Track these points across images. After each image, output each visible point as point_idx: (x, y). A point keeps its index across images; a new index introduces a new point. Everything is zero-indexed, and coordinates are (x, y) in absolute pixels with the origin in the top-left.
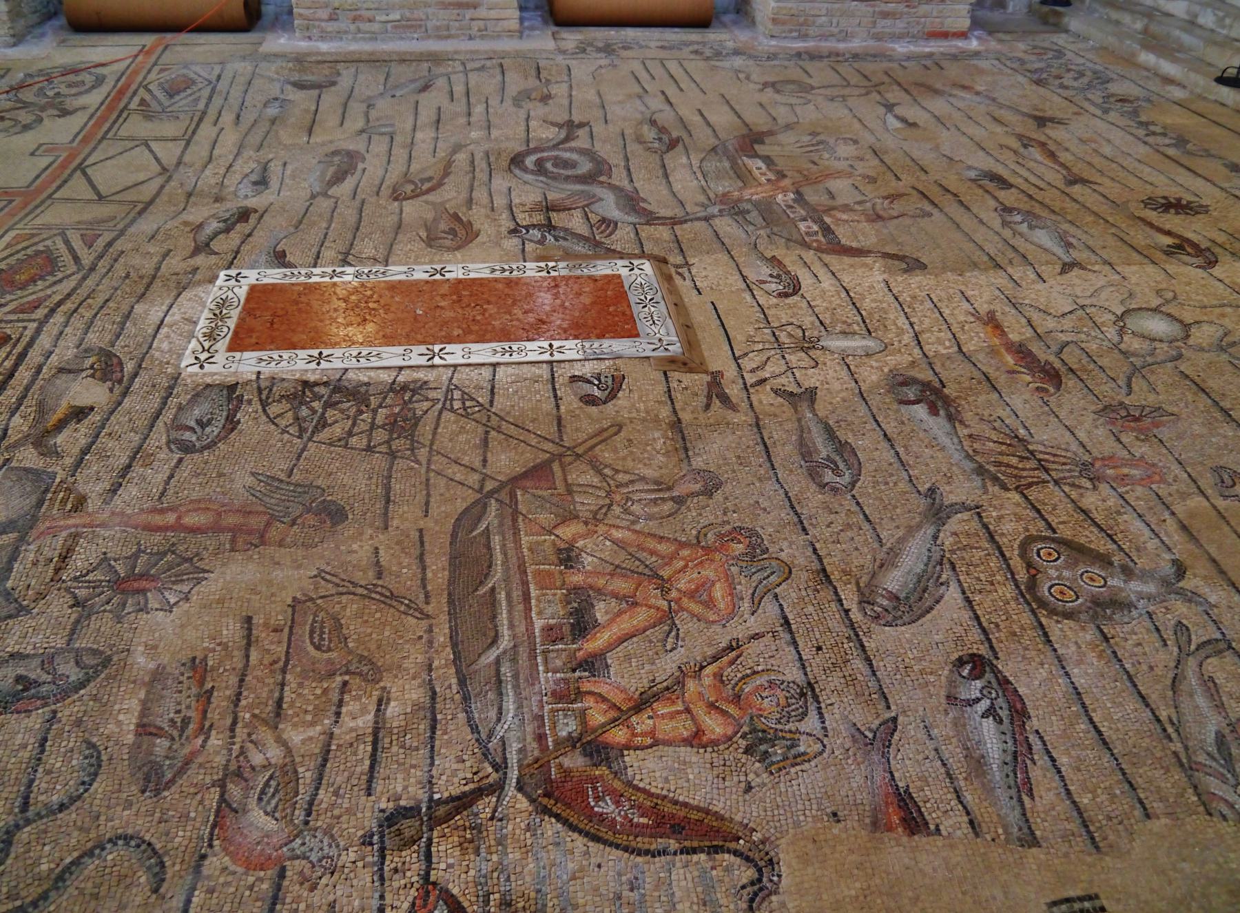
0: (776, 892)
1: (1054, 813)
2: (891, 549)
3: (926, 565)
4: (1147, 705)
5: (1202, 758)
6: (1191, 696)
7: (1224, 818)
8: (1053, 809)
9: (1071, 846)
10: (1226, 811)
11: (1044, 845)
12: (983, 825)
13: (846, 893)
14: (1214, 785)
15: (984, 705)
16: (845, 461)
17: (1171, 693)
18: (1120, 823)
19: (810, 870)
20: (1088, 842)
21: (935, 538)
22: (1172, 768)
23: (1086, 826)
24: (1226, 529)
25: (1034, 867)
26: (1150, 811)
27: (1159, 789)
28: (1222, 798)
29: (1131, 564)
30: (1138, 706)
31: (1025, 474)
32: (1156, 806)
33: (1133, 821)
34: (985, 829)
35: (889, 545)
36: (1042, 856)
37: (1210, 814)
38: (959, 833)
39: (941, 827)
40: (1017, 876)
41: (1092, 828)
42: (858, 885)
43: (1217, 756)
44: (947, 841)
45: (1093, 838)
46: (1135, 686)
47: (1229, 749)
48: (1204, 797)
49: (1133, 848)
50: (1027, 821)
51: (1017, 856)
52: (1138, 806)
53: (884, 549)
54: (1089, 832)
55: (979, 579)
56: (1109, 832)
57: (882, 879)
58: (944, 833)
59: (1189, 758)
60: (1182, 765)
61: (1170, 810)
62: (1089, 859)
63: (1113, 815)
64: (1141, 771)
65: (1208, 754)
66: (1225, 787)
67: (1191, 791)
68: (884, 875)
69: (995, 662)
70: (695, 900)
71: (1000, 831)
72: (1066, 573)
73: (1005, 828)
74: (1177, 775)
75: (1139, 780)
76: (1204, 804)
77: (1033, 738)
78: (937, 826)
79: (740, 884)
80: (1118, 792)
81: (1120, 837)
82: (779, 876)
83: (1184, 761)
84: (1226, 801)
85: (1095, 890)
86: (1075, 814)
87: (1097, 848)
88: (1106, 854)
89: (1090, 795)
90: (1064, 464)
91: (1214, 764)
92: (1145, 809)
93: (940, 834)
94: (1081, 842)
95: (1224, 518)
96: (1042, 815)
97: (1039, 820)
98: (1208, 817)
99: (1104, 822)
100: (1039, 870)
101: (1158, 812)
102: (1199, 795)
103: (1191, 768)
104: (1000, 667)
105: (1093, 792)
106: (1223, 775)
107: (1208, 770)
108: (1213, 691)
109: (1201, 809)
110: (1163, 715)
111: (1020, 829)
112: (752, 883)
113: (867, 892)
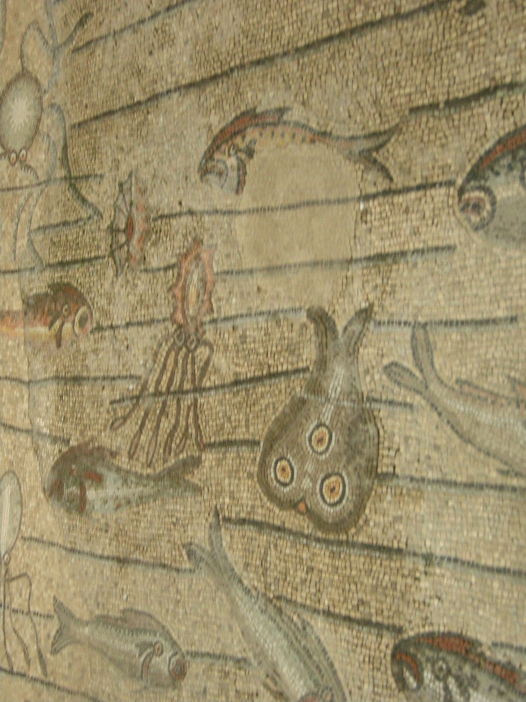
2: (255, 656)
3: (280, 629)
4: (481, 487)
6: (478, 424)
15: (452, 683)
16: (145, 631)
17: (469, 448)
21: (248, 592)
24: (278, 216)
29: (308, 375)
30: (480, 500)
31: (182, 423)
35: (250, 655)
46: (455, 484)
53: (255, 663)
55: (304, 581)
69: (405, 636)
72: (309, 467)
77: (500, 656)
90: (176, 362)
95: (263, 210)
104: (411, 633)
108: (475, 393)
110: (494, 477)
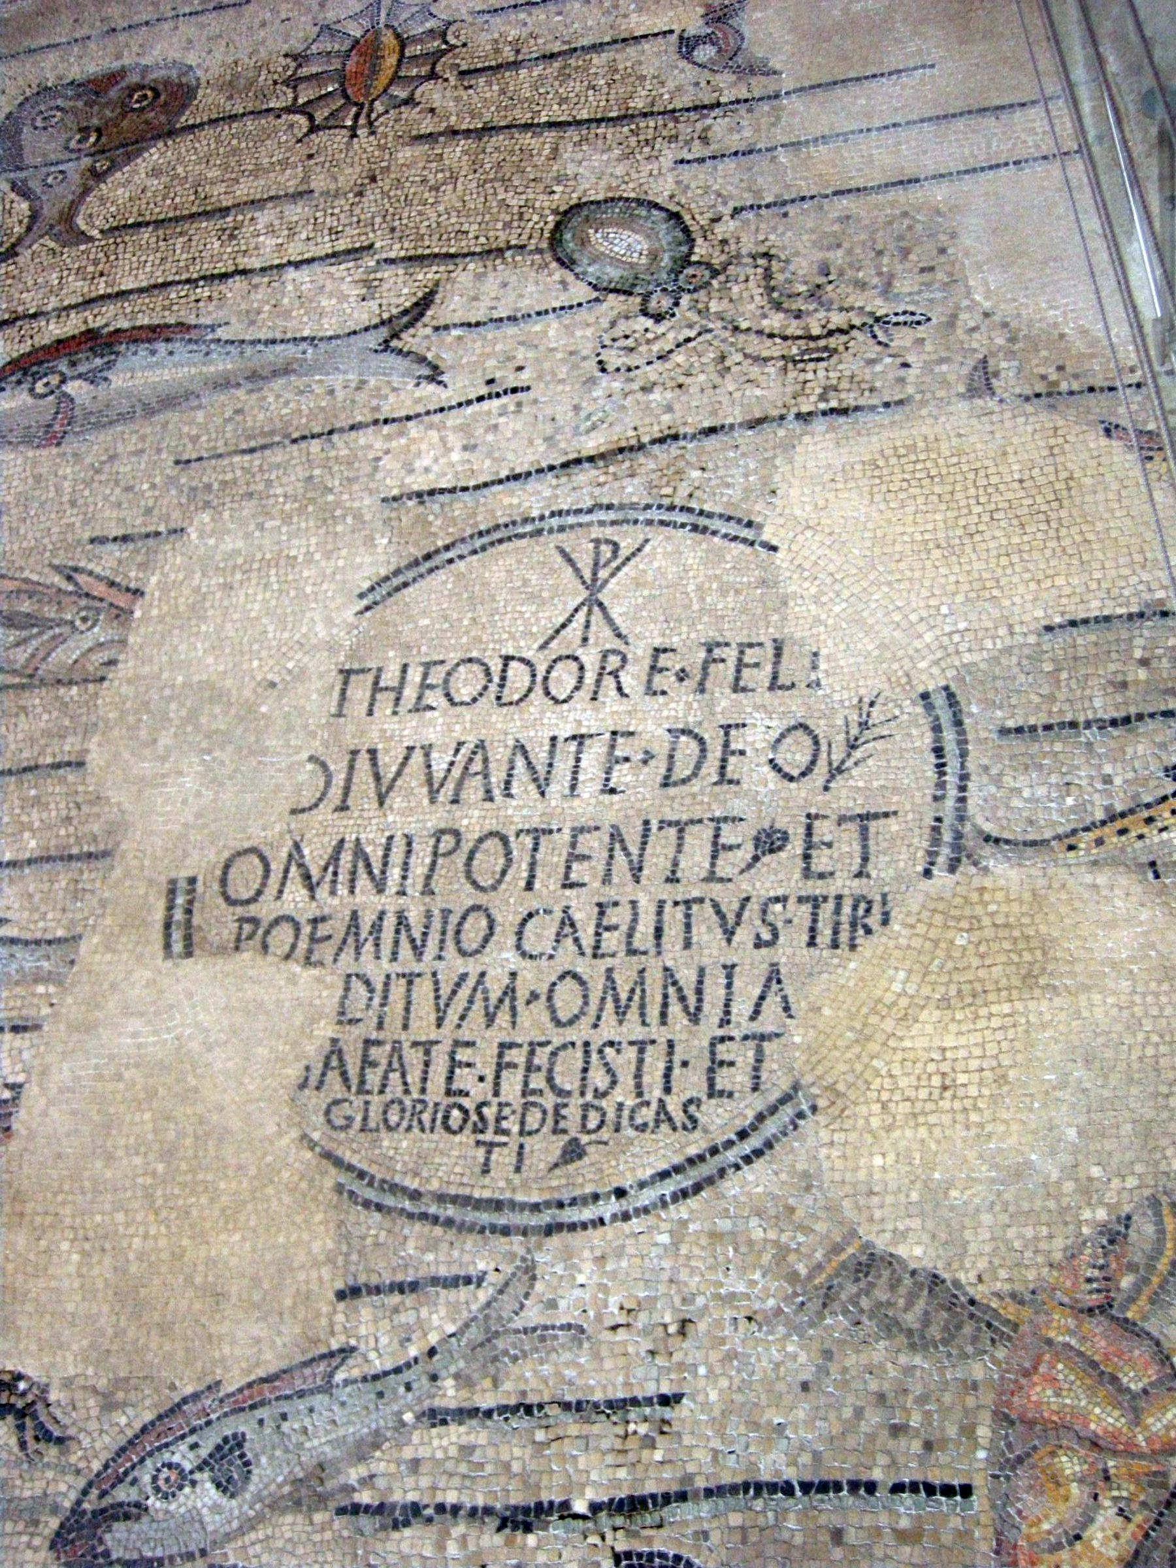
0: (45, 1389)
1: (37, 899)
5: (21, 656)
7: (112, 663)
8: (30, 896)
9: (92, 892)
10: (104, 656)
11: (79, 929)
12: (25, 1012)
13: (72, 1269)
14: (65, 656)
18: (78, 806)
19: (23, 1322)
20: (94, 864)
22: (22, 703)
23: (71, 857)
25: (108, 957)
26: (73, 758)
27: (47, 733)
28: (83, 655)
32: (69, 747)
33: (81, 788)
34: (33, 1013)
36: (95, 940)
37: (103, 679)
38: (26, 1055)
39: (11, 1080)
40: (113, 986)
41: (75, 851)
42: (65, 1246)
43: (25, 633)
44: (34, 1078)
45: (90, 855)
47: (19, 613)
48: (76, 677)
49: (119, 804)
50: (37, 942)
51: (85, 977)
52: (61, 771)
54: (78, 858)
56: (86, 828)
57: (64, 1203)
58: (20, 1078)
59: (14, 672)
60: (23, 687)
61: (80, 730)
62: (118, 873)
63: (64, 813)
64: (13, 747)
65: (18, 645)
66: (71, 643)
67: (62, 691)
68: (60, 1198)
70: (25, 1538)
71: (41, 989)
73: (37, 980)
74: (34, 699)
75: (26, 754)
76: (86, 681)
78: (6, 1086)
79: (16, 1449)
80: (33, 792)
81: (98, 815)
82: (19, 1377)
83: (17, 680)
84: (90, 650)
85: (163, 879)
86: (47, 866)
87: (105, 854)
88: (118, 844)
89: (27, 835)
91: (35, 643)
92: (69, 764)
93: (20, 1086)
94: (88, 875)
96: (36, 916)
97: (41, 924)
98: (106, 684)
99: (71, 829)
100: (114, 951)
101: (78, 747)
102: (71, 683)
103: (31, 676)
105: (24, 827)
106: (54, 638)
107: (41, 654)
109: (91, 687)
111: (48, 958)
112: (21, 1428)
113: (81, 1232)
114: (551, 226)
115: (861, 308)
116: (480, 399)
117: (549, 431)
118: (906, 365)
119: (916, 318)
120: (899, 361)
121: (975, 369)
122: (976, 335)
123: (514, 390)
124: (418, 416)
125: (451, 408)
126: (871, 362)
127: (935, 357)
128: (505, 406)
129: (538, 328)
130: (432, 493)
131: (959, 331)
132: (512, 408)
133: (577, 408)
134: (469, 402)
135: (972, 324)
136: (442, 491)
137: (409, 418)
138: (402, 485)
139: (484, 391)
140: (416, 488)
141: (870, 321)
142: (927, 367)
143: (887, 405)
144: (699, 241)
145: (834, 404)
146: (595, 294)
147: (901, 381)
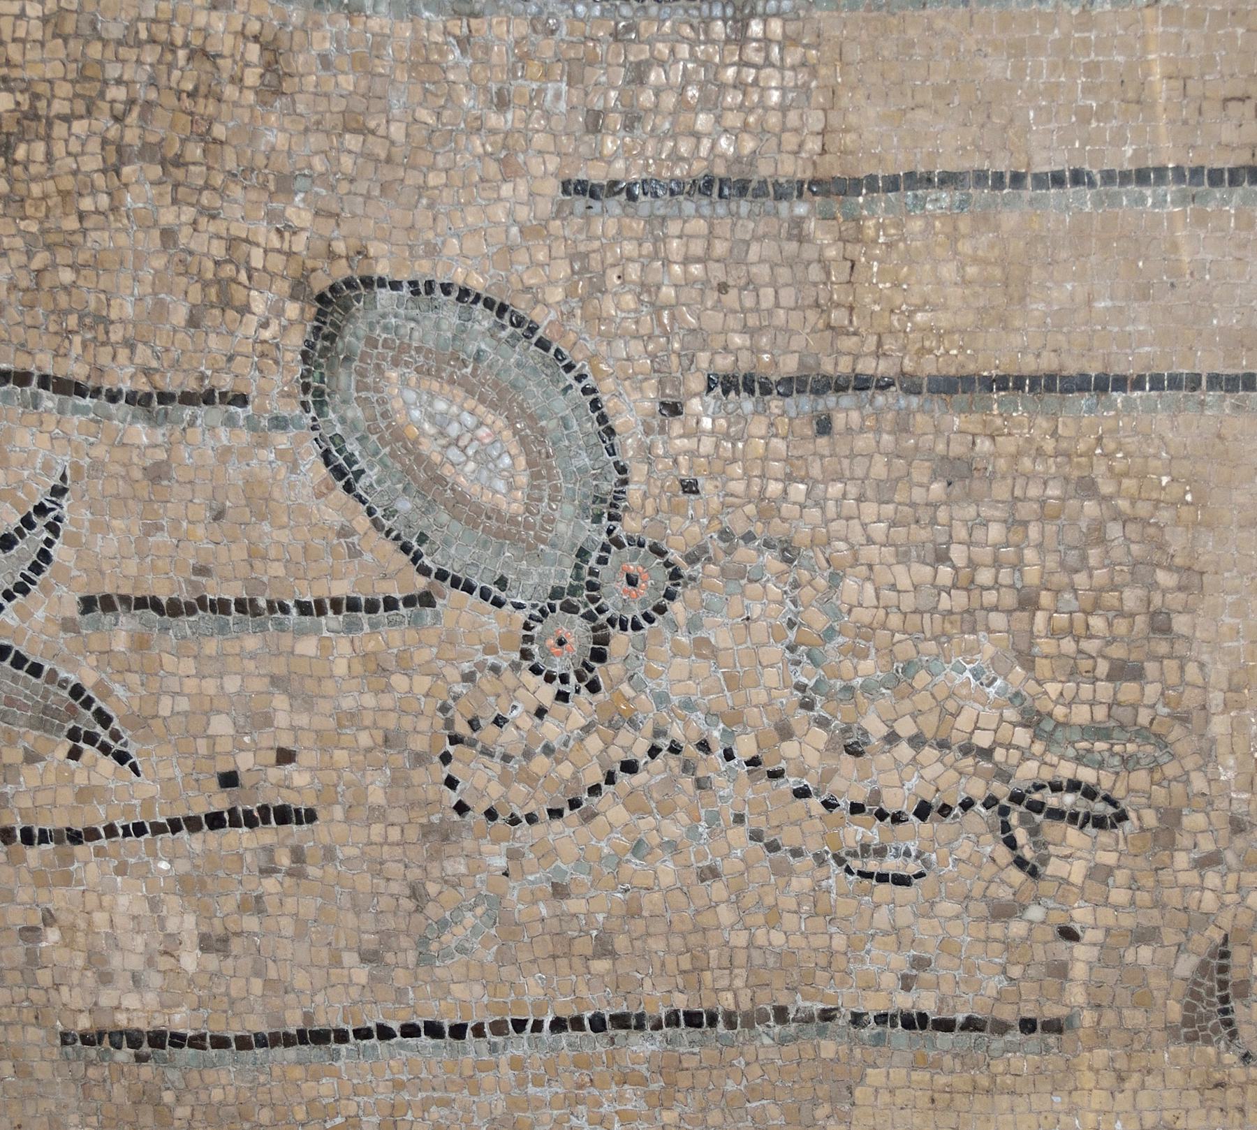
114: (296, 340)
115: (987, 753)
116: (215, 821)
117: (370, 940)
118: (1068, 934)
119: (1099, 807)
120: (1059, 918)
121: (1203, 968)
122: (1212, 878)
123: (284, 815)
124: (92, 834)
125: (158, 829)
126: (1003, 912)
127: (1127, 921)
128: (269, 851)
129: (308, 646)
130: (157, 1039)
131: (1182, 859)
132: (285, 860)
133: (416, 893)
134: (193, 824)
135: (1207, 845)
136: (178, 1040)
137: (76, 837)
138: (94, 1009)
139: (220, 802)
140: (122, 1020)
141: (1002, 791)
142: (1108, 954)
143: (1028, 1026)
144: (638, 473)
145: (927, 1003)
146: (421, 583)
147: (1060, 971)
